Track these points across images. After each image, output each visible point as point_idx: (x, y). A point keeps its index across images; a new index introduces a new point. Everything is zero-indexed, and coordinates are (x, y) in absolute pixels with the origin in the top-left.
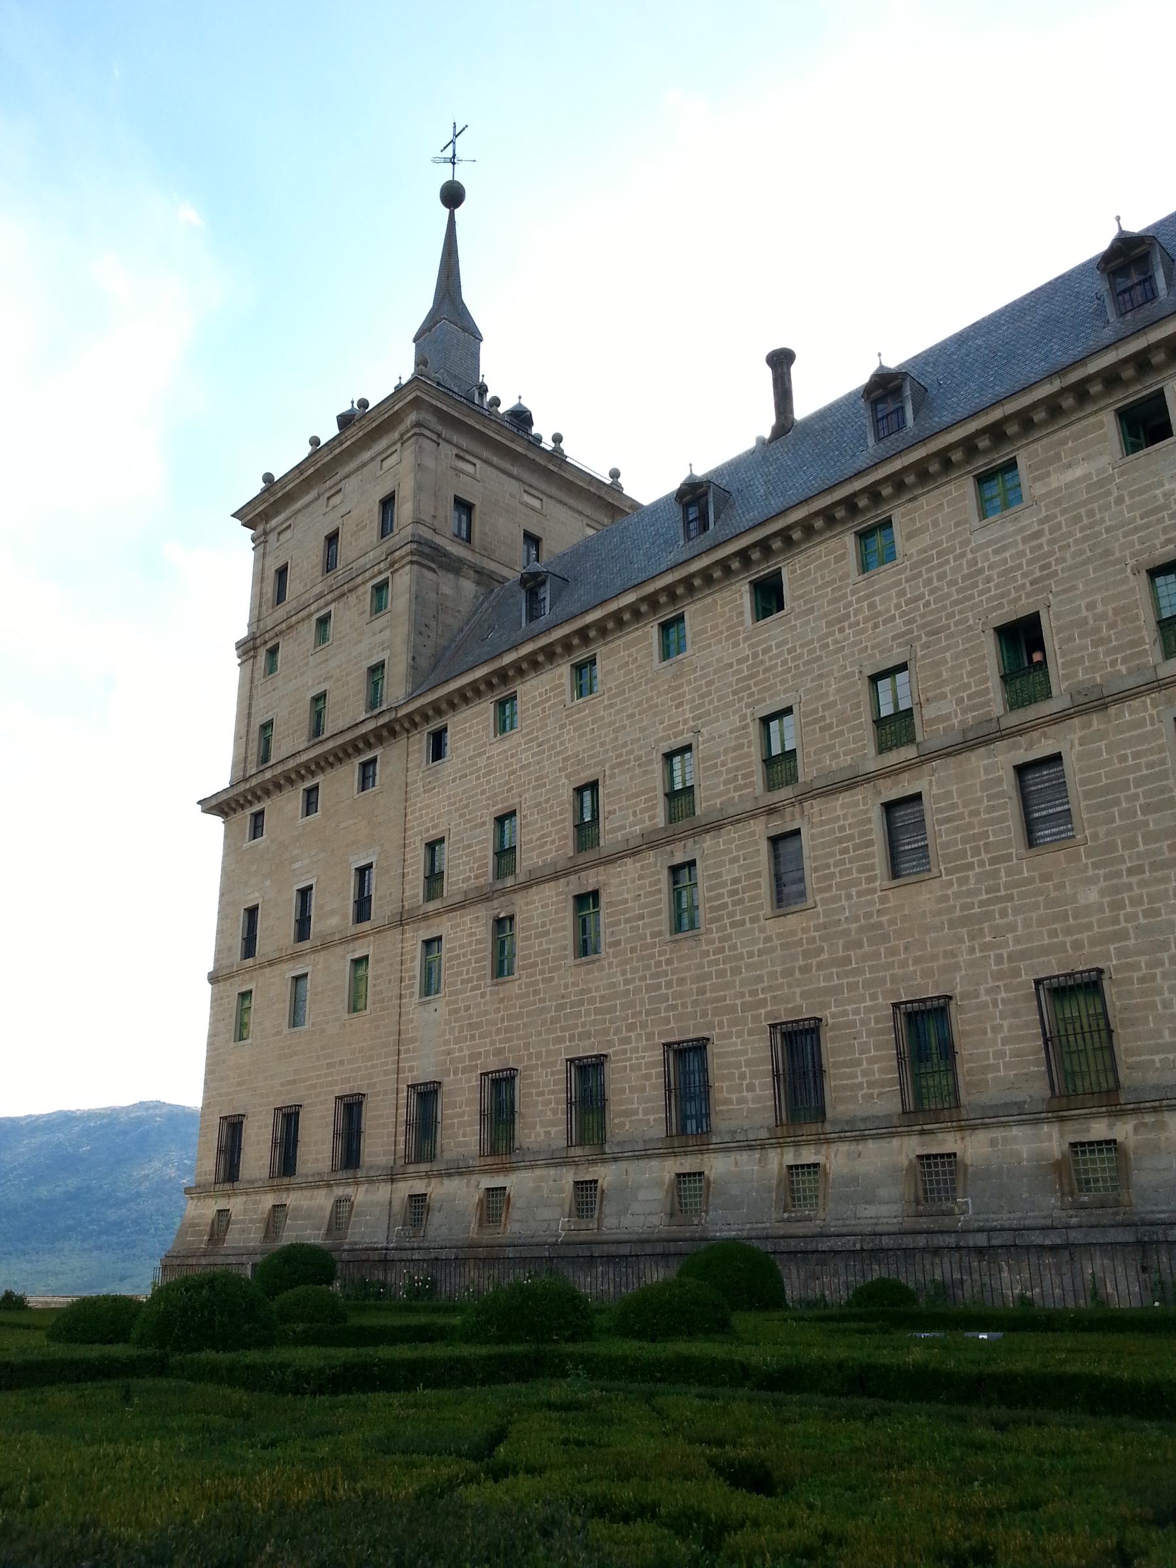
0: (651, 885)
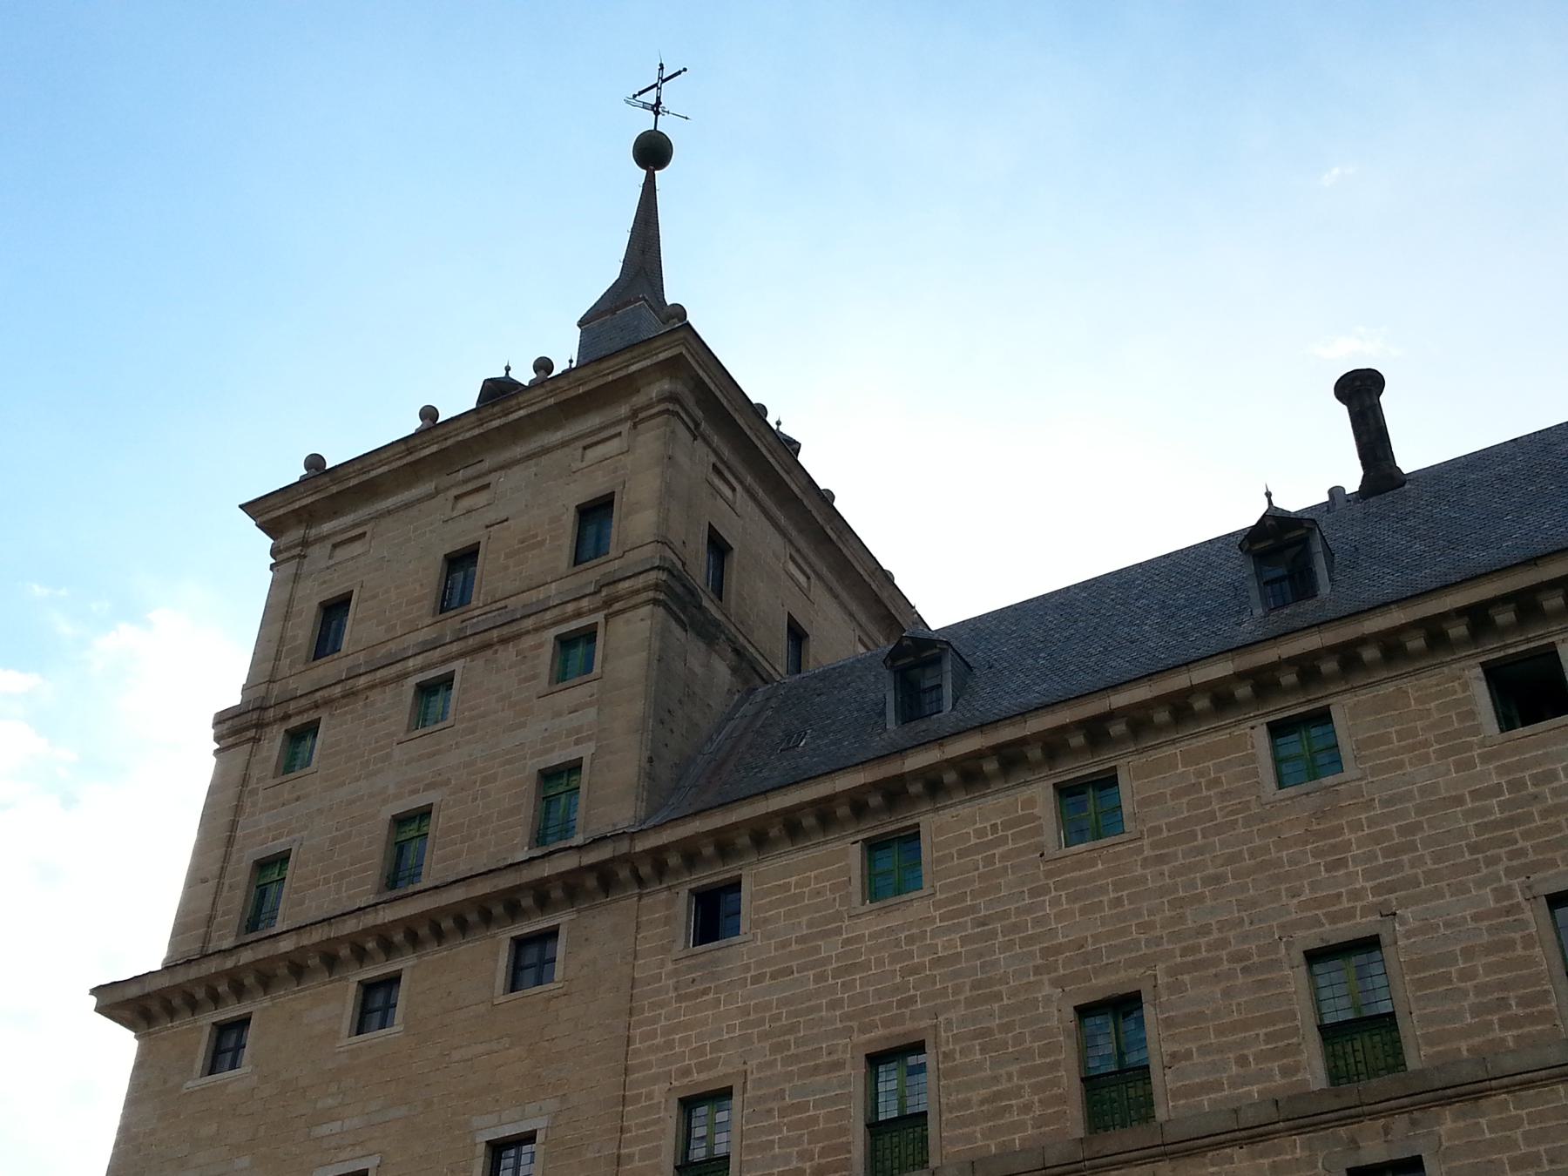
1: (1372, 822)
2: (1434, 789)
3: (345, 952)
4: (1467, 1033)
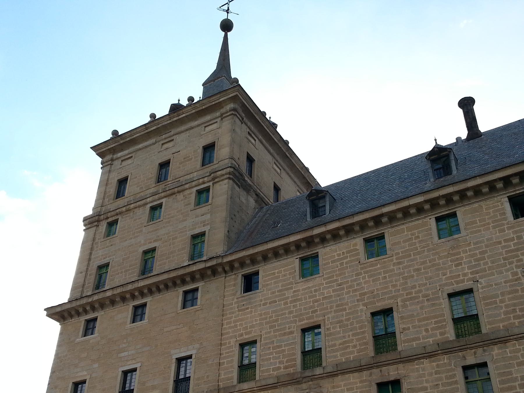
0: (447, 378)
1: (470, 250)
2: (491, 239)
3: (128, 296)
4: (502, 321)
